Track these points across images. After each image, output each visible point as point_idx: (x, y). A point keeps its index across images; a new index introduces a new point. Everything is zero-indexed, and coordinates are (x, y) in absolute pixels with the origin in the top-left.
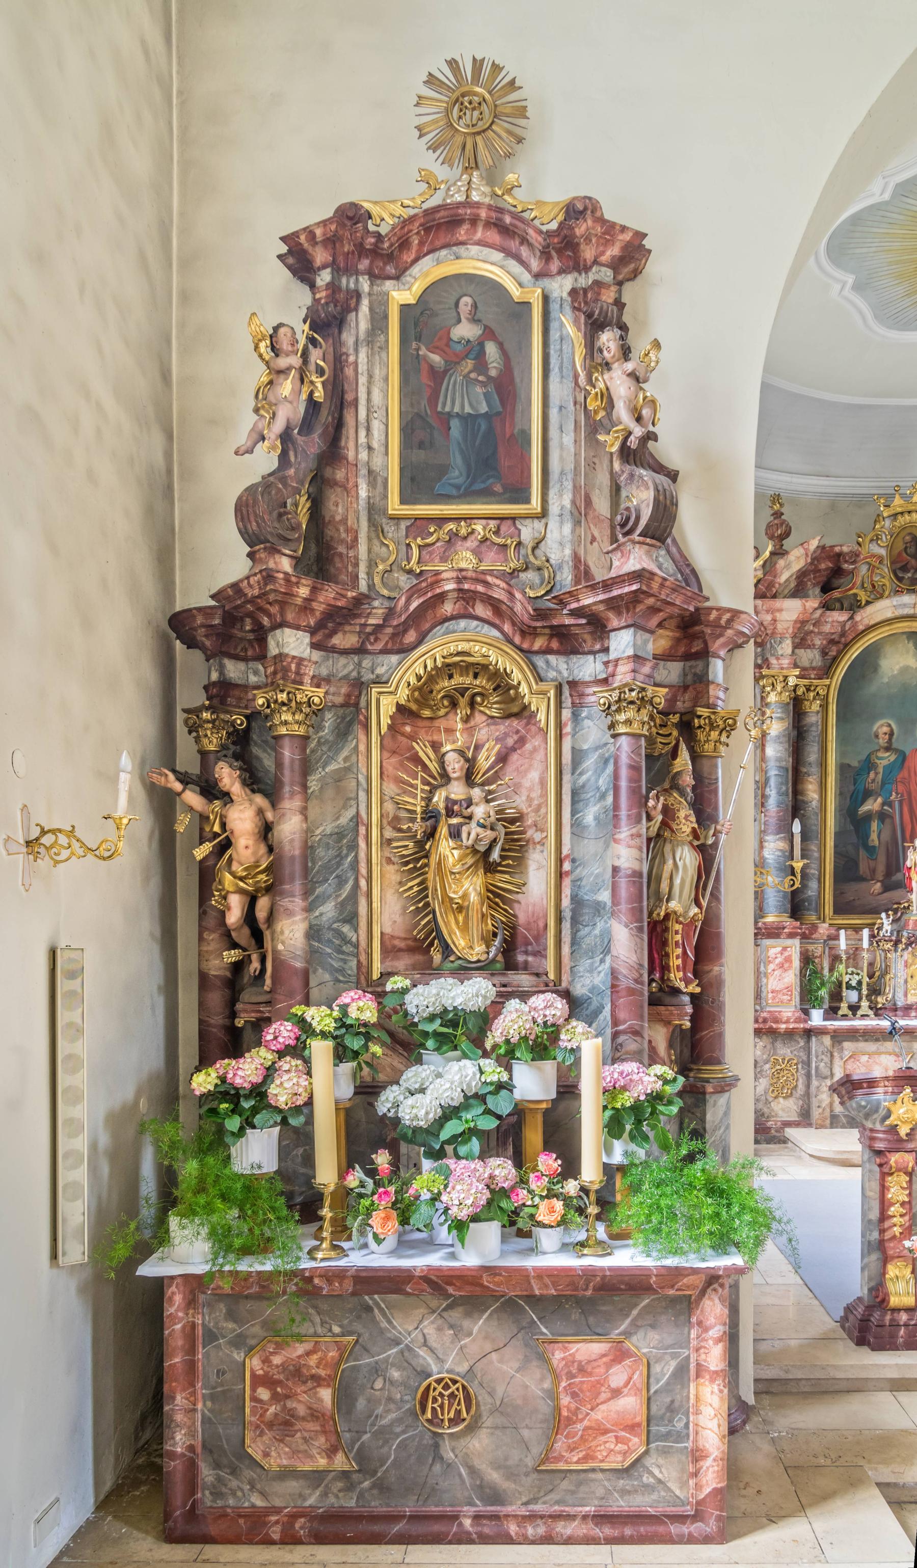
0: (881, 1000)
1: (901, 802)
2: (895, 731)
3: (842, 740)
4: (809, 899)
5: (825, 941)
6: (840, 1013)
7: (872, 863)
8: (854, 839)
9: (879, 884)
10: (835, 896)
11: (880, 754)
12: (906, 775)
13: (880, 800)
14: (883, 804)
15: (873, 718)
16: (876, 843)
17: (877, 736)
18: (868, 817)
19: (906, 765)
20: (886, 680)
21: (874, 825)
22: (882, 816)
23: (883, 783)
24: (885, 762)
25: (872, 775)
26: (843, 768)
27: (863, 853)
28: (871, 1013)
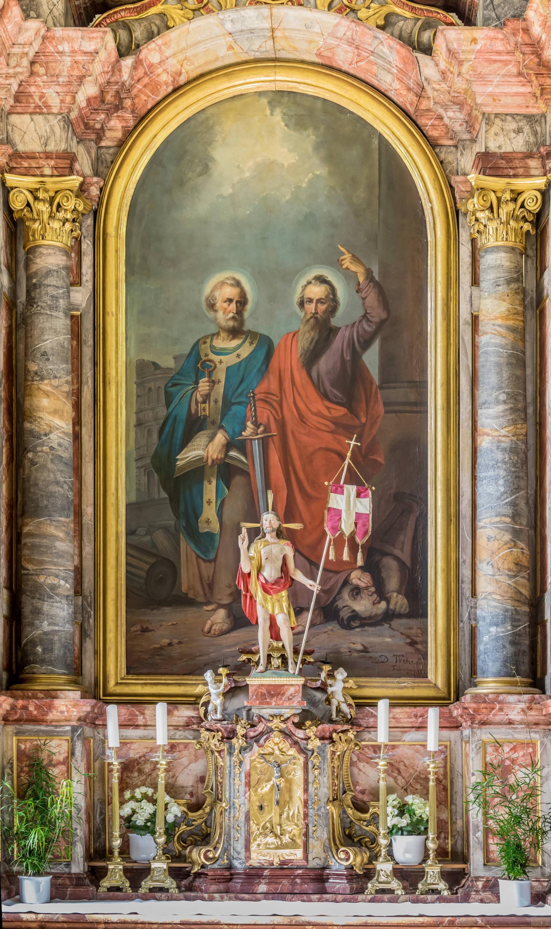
0: (197, 855)
1: (265, 444)
2: (250, 296)
3: (141, 312)
4: (46, 640)
5: (74, 729)
6: (106, 883)
7: (207, 569)
8: (168, 518)
9: (221, 613)
10: (130, 638)
11: (220, 343)
12: (274, 386)
13: (220, 438)
14: (228, 446)
15: (206, 268)
16: (215, 526)
17: (212, 306)
18: (198, 472)
19: (274, 363)
20: (227, 190)
21: (210, 489)
22: (227, 472)
23: (227, 404)
24: (230, 360)
25: (203, 385)
26: (143, 372)
27: (186, 547)
28: (170, 883)
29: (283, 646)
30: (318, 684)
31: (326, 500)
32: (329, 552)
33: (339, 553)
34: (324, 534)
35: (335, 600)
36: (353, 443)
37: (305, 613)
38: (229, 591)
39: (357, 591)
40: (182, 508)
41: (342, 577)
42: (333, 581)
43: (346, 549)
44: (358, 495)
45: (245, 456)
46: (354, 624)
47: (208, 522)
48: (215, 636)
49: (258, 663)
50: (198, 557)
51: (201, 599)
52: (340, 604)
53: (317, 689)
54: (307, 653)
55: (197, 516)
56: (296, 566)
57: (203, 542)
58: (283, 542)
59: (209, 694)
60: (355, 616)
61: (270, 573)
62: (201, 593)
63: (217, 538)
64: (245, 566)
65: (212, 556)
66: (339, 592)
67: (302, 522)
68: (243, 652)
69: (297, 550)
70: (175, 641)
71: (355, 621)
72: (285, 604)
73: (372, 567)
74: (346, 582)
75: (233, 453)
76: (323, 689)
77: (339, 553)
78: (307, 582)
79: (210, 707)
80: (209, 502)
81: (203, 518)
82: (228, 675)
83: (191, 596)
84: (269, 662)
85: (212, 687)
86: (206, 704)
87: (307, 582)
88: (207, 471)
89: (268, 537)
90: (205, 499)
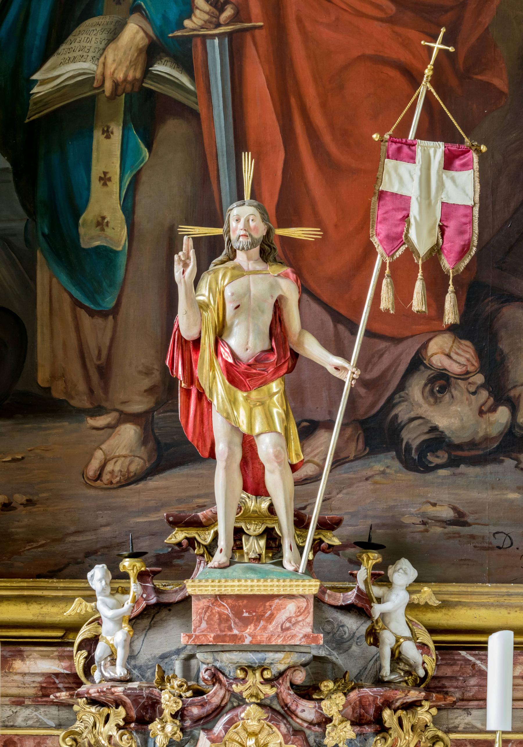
9: (129, 433)
16: (118, 235)
18: (79, 111)
21: (108, 150)
22: (147, 110)
29: (271, 509)
30: (351, 597)
31: (374, 174)
32: (380, 293)
33: (403, 295)
34: (369, 252)
35: (390, 404)
36: (437, 46)
37: (321, 435)
38: (146, 383)
39: (441, 383)
40: (42, 192)
41: (407, 351)
42: (386, 361)
43: (419, 286)
44: (449, 163)
45: (189, 70)
46: (433, 459)
47: (101, 223)
48: (111, 487)
49: (211, 549)
50: (77, 303)
51: (81, 401)
52: (402, 412)
53: (347, 609)
54: (326, 525)
55: (77, 212)
56: (304, 326)
57: (90, 268)
58: (275, 270)
59: (98, 621)
60: (437, 440)
61: (245, 340)
62: (82, 387)
63: (122, 260)
64: (186, 324)
65: (109, 303)
66: (402, 386)
67: (318, 223)
68: (177, 522)
69: (305, 290)
70: (19, 498)
71: (437, 452)
72: (277, 412)
73: (475, 328)
74: (417, 363)
75: (161, 68)
76: (361, 609)
77: (403, 295)
78: (330, 361)
79: (100, 651)
80: (105, 179)
81: (89, 215)
82: (142, 576)
83: (57, 394)
84: (238, 547)
85: (105, 605)
86: (91, 643)
87: (330, 361)
88: (102, 107)
89: (241, 258)
90: (96, 171)
